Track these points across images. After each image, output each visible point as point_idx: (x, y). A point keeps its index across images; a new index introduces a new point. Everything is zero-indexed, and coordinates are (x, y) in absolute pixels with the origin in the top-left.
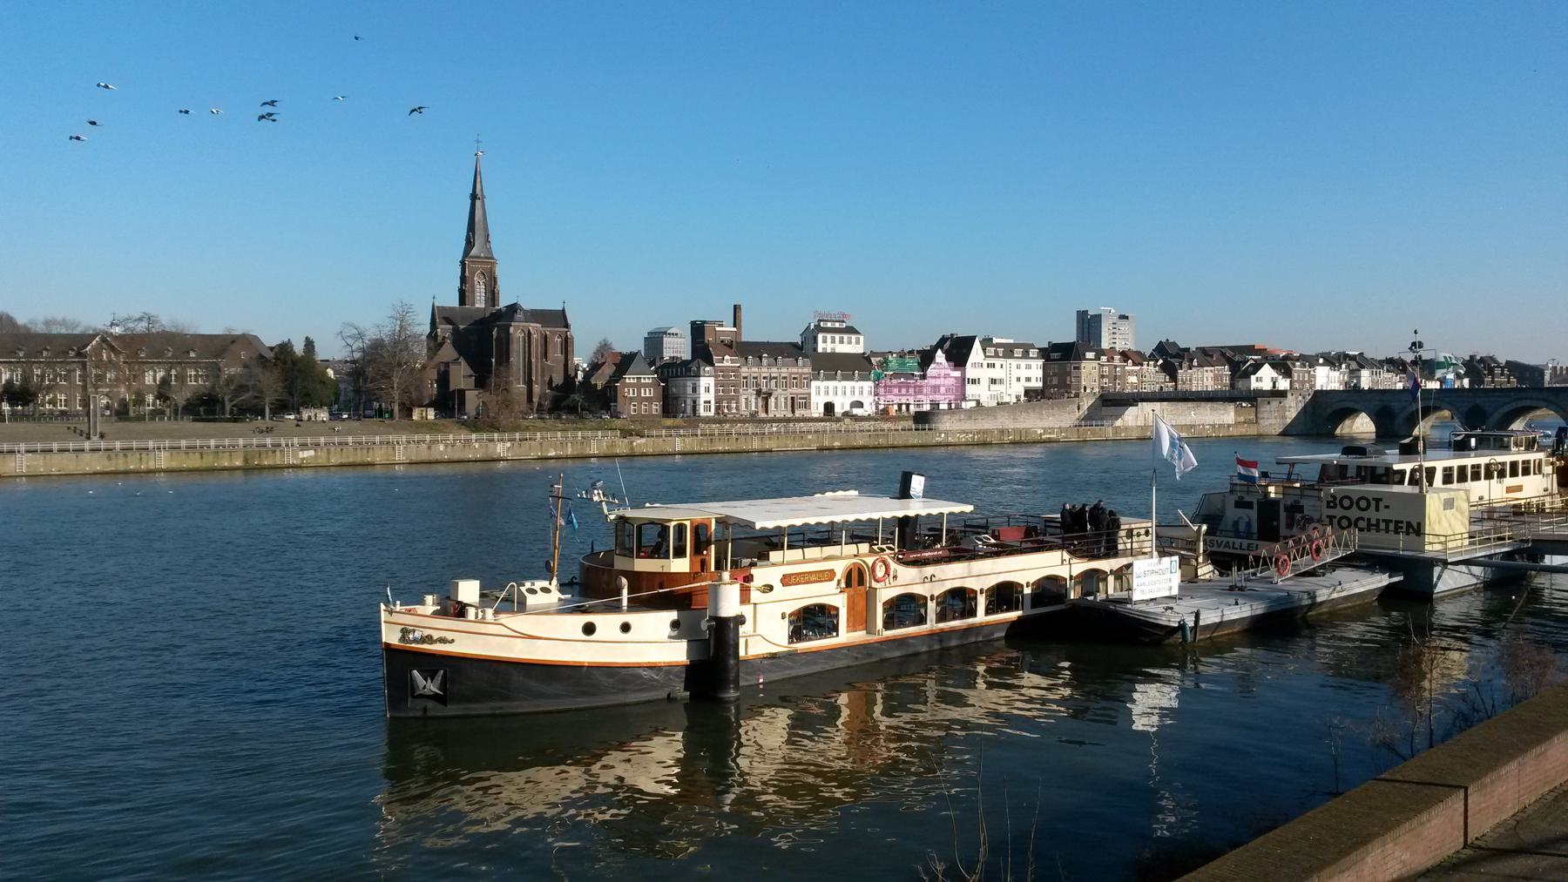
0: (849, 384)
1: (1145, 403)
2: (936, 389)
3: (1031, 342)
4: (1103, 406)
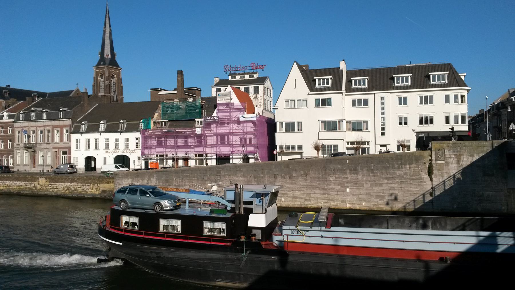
0: (112, 136)
2: (223, 139)
3: (446, 62)
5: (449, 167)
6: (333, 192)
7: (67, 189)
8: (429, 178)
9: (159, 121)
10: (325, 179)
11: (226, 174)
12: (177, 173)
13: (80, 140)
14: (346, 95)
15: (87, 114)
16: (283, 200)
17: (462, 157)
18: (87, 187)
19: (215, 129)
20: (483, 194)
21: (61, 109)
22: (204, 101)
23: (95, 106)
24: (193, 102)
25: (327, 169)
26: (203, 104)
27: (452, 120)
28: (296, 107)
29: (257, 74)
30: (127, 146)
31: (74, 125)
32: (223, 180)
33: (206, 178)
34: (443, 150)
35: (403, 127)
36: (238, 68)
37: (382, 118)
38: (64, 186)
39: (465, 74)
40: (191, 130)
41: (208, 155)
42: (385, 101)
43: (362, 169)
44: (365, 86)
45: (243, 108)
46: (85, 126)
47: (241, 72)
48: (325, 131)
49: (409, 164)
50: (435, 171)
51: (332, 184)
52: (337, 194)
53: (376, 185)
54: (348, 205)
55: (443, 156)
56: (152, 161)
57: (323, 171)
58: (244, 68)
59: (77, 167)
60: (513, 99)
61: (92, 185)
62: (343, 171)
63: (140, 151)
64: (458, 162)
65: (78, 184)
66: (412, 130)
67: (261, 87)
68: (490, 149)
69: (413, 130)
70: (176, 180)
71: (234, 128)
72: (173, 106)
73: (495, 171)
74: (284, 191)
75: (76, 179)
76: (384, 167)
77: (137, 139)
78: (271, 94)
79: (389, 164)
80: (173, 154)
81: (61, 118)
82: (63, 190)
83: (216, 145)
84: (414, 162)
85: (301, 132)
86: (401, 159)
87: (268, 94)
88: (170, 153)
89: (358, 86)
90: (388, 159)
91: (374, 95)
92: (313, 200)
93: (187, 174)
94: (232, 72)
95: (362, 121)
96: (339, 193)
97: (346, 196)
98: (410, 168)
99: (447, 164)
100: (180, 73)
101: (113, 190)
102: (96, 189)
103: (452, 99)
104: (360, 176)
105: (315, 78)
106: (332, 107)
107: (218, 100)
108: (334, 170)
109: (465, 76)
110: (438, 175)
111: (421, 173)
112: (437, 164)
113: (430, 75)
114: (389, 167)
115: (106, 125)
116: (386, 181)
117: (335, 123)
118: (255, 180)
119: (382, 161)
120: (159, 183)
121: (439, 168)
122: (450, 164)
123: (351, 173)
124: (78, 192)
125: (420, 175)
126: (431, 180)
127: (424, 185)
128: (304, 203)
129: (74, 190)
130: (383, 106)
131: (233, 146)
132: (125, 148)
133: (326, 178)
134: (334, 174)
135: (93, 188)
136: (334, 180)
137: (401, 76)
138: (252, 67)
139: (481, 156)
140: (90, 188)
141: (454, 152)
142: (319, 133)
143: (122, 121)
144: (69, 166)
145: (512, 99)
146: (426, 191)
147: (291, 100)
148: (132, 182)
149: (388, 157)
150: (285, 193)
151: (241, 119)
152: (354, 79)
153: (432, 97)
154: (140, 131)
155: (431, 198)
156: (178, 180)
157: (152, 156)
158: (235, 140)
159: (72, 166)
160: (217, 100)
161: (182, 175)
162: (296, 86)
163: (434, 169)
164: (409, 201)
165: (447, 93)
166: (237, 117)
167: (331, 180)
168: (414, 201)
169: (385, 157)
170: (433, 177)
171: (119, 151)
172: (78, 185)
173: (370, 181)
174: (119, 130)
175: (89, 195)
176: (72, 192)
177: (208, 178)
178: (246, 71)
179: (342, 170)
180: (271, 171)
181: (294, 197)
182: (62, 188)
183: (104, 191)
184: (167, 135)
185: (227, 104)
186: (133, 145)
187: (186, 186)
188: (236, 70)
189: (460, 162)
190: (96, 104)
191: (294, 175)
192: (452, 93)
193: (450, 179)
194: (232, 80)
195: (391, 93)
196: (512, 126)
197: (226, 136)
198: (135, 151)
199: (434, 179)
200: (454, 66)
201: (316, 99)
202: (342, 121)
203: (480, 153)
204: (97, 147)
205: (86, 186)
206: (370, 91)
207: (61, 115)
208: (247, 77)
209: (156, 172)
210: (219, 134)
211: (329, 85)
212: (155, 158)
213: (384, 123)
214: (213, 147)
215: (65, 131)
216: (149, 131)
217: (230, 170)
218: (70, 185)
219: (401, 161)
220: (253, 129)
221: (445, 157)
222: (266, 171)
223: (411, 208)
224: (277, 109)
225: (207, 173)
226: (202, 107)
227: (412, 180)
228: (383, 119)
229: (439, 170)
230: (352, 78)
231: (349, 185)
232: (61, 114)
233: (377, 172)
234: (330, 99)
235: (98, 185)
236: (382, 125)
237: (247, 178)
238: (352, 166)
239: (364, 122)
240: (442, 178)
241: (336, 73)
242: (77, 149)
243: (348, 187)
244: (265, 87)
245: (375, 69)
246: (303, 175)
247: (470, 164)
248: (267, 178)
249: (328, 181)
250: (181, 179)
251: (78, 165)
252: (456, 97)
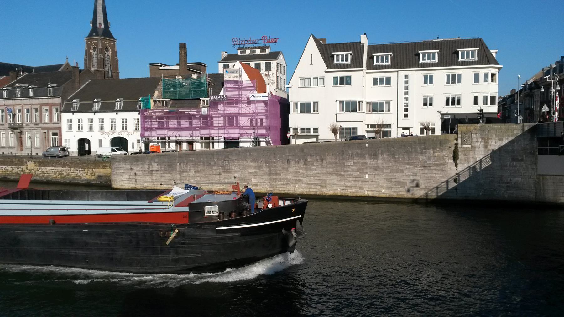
0: (107, 116)
2: (231, 121)
3: (476, 37)
4: (542, 152)
5: (476, 152)
6: (351, 179)
7: (59, 174)
8: (454, 164)
9: (160, 100)
10: (343, 165)
11: (234, 158)
12: (181, 157)
13: (71, 120)
14: (366, 73)
15: (78, 91)
16: (297, 187)
17: (490, 141)
18: (82, 172)
19: (223, 109)
20: (511, 180)
21: (49, 86)
22: (209, 78)
23: (87, 83)
24: (197, 79)
25: (345, 154)
26: (209, 81)
27: (481, 101)
28: (312, 86)
29: (269, 48)
30: (124, 127)
31: (64, 104)
32: (231, 165)
33: (213, 163)
34: (470, 133)
35: (428, 108)
36: (247, 41)
37: (405, 98)
38: (56, 171)
39: (497, 51)
40: (195, 110)
41: (215, 138)
42: (409, 80)
43: (382, 154)
44: (388, 63)
45: (254, 87)
46: (77, 105)
47: (251, 46)
48: (343, 112)
49: (433, 149)
50: (461, 156)
51: (350, 170)
52: (355, 181)
53: (397, 170)
54: (366, 192)
55: (470, 139)
56: (153, 144)
57: (341, 156)
58: (255, 42)
59: (69, 150)
60: (547, 78)
61: (86, 170)
62: (362, 156)
63: (139, 133)
64: (486, 146)
65: (71, 168)
66: (438, 111)
67: (274, 63)
68: (520, 133)
69: (439, 112)
70: (179, 165)
71: (244, 108)
72: (176, 84)
73: (524, 156)
74: (298, 177)
75: (68, 163)
76: (406, 152)
77: (135, 119)
78: (284, 71)
79: (412, 149)
80: (176, 137)
81: (50, 95)
82: (54, 175)
83: (224, 126)
84: (438, 146)
85: (317, 113)
86: (424, 143)
87: (281, 71)
88: (172, 135)
89: (380, 63)
90: (411, 142)
91: (397, 73)
92: (330, 187)
93: (192, 159)
94: (241, 46)
95: (383, 102)
96: (357, 179)
97: (364, 183)
98: (434, 152)
99: (473, 148)
100: (183, 46)
101: (110, 175)
102: (91, 174)
103: (481, 78)
104: (380, 162)
105: (333, 53)
106: (351, 86)
107: (226, 77)
108: (352, 154)
109: (496, 52)
110: (463, 160)
111: (445, 158)
112: (463, 148)
113: (459, 51)
114: (411, 152)
115: (100, 104)
116: (408, 167)
117: (354, 103)
118: (266, 165)
119: (404, 146)
120: (161, 168)
121: (465, 153)
122: (477, 148)
123: (370, 158)
124: (71, 177)
125: (444, 160)
126: (456, 165)
127: (448, 171)
128: (320, 190)
129: (66, 175)
130: (407, 85)
131: (242, 128)
132: (123, 129)
133: (344, 163)
134: (353, 159)
135: (88, 173)
136: (352, 166)
137: (427, 52)
138: (264, 41)
139: (511, 140)
140: (84, 173)
141: (481, 135)
142: (336, 114)
143: (118, 100)
144: (60, 148)
145: (546, 78)
146: (450, 177)
147: (306, 78)
148: (131, 167)
149: (411, 141)
150: (299, 179)
151: (252, 99)
152: (375, 56)
153: (460, 76)
154: (139, 111)
155: (456, 184)
156: (182, 165)
157: (153, 138)
158: (244, 121)
159: (63, 149)
160: (225, 77)
161: (186, 160)
162: (312, 62)
163: (459, 153)
164: (432, 188)
165: (476, 71)
166: (247, 96)
167: (348, 166)
168: (437, 188)
169: (407, 141)
170: (458, 162)
171: (116, 132)
172: (71, 170)
173: (390, 167)
174: (115, 110)
175: (83, 180)
176: (65, 177)
177: (215, 163)
178: (257, 45)
179: (361, 154)
180: (284, 156)
181: (308, 184)
182: (53, 172)
183: (100, 177)
184: (169, 116)
185: (236, 82)
186: (131, 126)
187: (191, 172)
188: (246, 44)
189: (488, 147)
190: (89, 80)
191: (309, 160)
192: (483, 70)
193: (477, 164)
194: (241, 55)
195: (415, 71)
196: (545, 108)
197: (235, 118)
198: (133, 133)
199: (459, 165)
200: (485, 41)
201: (334, 77)
202: (362, 102)
203: (509, 137)
204: (91, 128)
205: (79, 170)
206: (393, 69)
207: (50, 92)
208: (258, 52)
209: (158, 156)
210: (227, 114)
211: (348, 61)
212: (156, 141)
213: (407, 103)
214: (220, 129)
215: (54, 110)
216: (149, 111)
217: (240, 154)
218: (62, 170)
219: (424, 145)
220: (265, 110)
221: (472, 141)
222: (279, 155)
223: (433, 195)
224: (291, 87)
225: (214, 158)
226: (208, 85)
227: (435, 165)
228: (407, 99)
229: (465, 155)
230: (373, 54)
231: (368, 170)
232: (49, 91)
233: (398, 157)
234: (350, 77)
235: (94, 169)
236: (405, 106)
237: (258, 163)
238: (372, 150)
239: (386, 102)
240: (467, 163)
241: (356, 48)
242: (69, 130)
243: (367, 173)
244: (278, 63)
245: (399, 44)
246: (318, 160)
247: (498, 149)
248: (280, 163)
249: (346, 167)
250: (185, 164)
251: (70, 148)
252: (486, 75)
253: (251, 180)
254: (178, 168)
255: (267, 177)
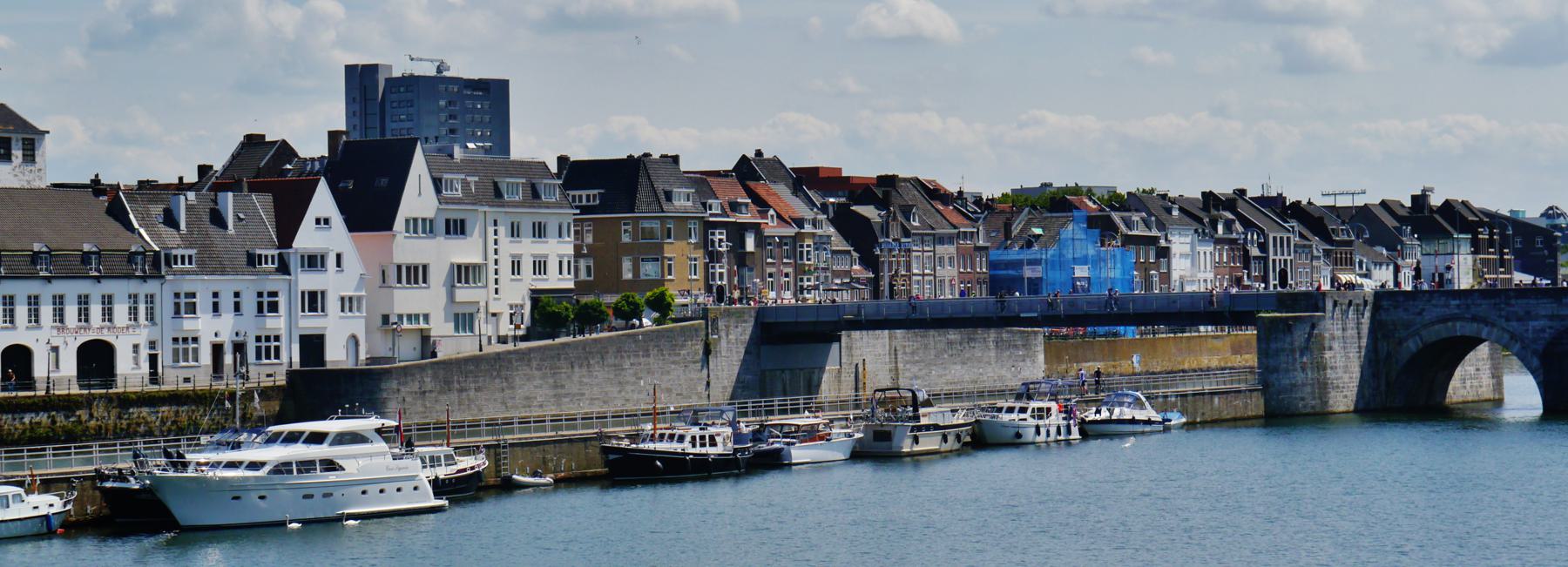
1: (856, 334)
2: (314, 301)
116: (673, 366)
134: (629, 357)
222: (563, 356)
253: (536, 398)
254: (456, 386)
255: (551, 392)
